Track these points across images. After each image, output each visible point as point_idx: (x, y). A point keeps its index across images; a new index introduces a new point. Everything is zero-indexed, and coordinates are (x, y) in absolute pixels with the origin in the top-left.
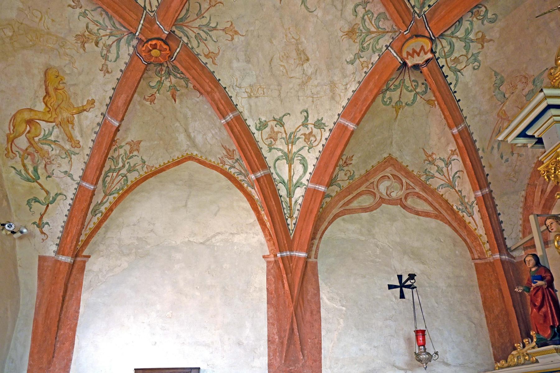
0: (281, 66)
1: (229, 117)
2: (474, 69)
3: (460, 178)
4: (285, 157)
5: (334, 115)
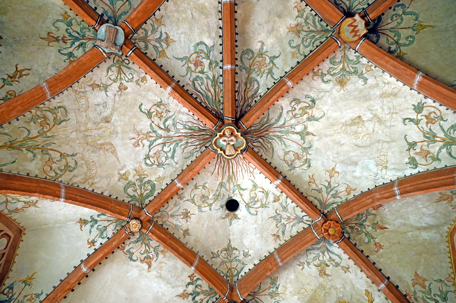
0: (363, 138)
1: (397, 191)
4: (449, 146)
5: (411, 93)
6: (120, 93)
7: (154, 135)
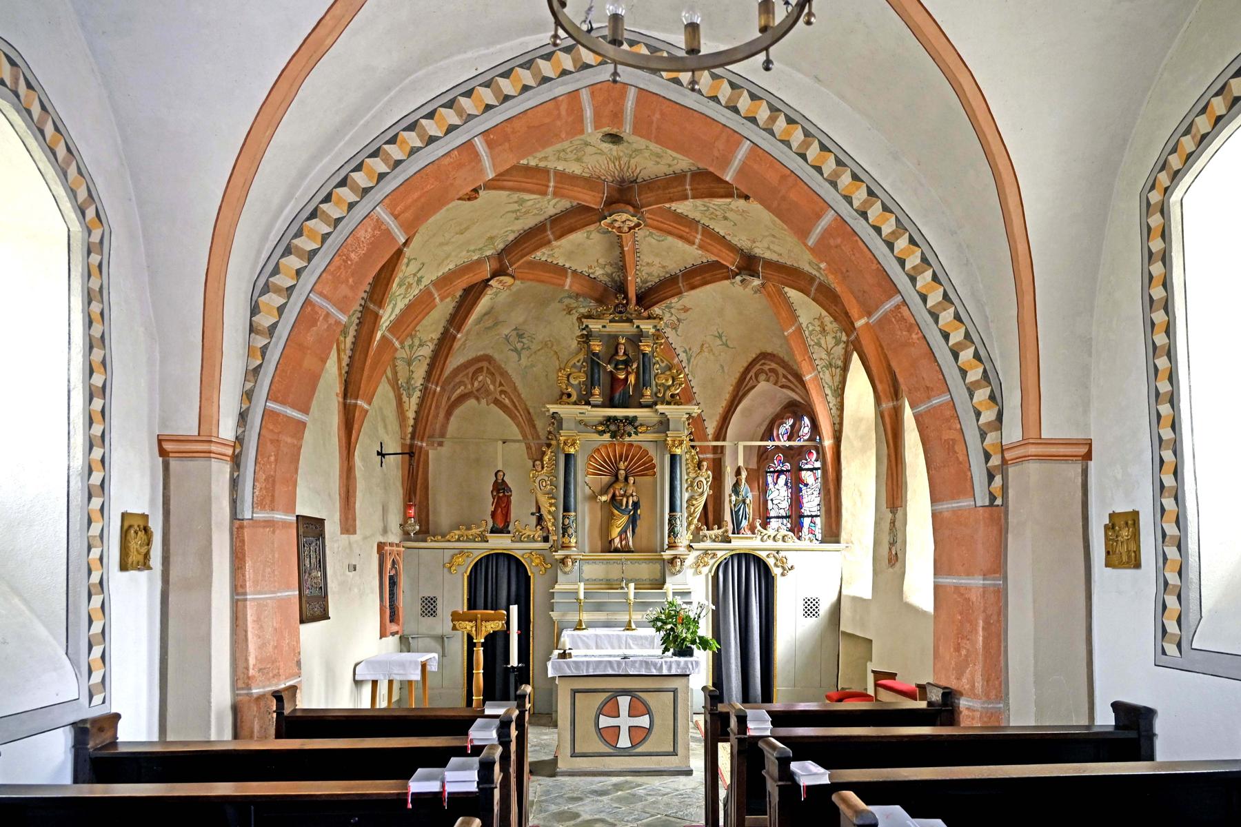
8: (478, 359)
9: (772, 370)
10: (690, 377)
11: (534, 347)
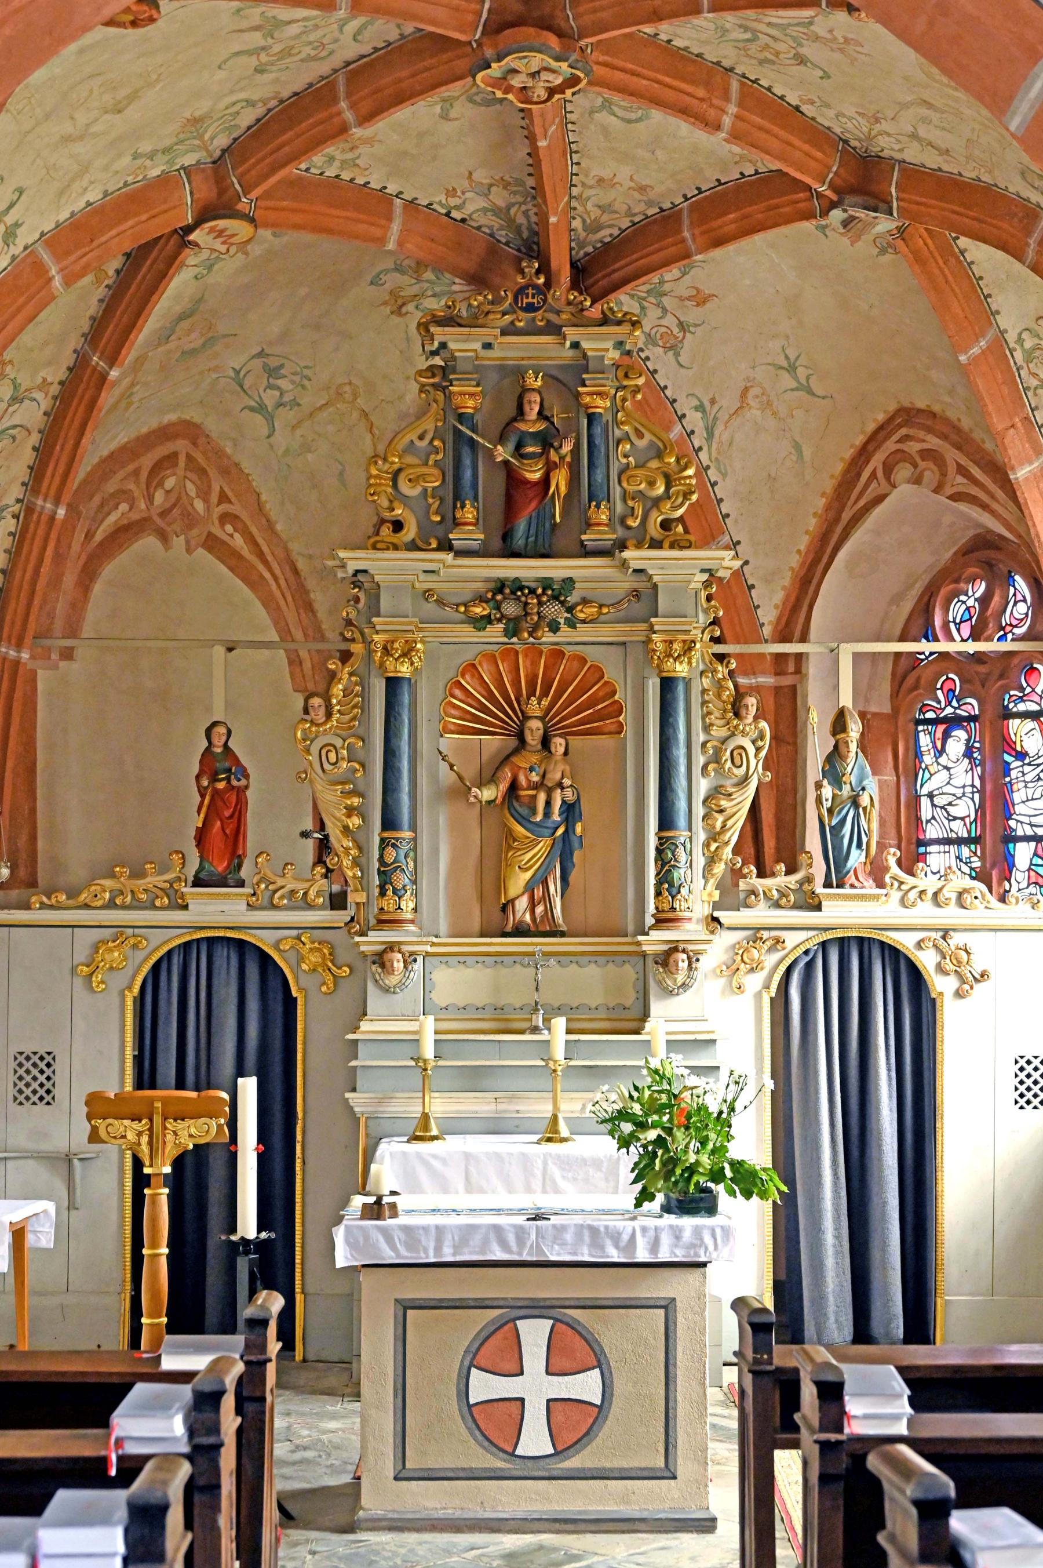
2: (196, 277)
3: (14, 441)
6: (879, 115)
7: (794, 34)
8: (164, 434)
9: (927, 454)
10: (713, 474)
11: (307, 400)
